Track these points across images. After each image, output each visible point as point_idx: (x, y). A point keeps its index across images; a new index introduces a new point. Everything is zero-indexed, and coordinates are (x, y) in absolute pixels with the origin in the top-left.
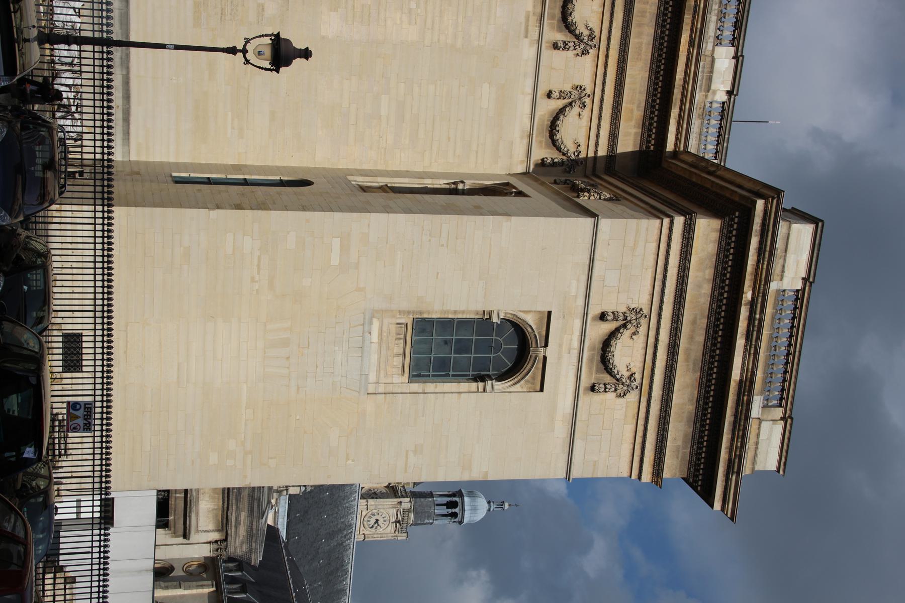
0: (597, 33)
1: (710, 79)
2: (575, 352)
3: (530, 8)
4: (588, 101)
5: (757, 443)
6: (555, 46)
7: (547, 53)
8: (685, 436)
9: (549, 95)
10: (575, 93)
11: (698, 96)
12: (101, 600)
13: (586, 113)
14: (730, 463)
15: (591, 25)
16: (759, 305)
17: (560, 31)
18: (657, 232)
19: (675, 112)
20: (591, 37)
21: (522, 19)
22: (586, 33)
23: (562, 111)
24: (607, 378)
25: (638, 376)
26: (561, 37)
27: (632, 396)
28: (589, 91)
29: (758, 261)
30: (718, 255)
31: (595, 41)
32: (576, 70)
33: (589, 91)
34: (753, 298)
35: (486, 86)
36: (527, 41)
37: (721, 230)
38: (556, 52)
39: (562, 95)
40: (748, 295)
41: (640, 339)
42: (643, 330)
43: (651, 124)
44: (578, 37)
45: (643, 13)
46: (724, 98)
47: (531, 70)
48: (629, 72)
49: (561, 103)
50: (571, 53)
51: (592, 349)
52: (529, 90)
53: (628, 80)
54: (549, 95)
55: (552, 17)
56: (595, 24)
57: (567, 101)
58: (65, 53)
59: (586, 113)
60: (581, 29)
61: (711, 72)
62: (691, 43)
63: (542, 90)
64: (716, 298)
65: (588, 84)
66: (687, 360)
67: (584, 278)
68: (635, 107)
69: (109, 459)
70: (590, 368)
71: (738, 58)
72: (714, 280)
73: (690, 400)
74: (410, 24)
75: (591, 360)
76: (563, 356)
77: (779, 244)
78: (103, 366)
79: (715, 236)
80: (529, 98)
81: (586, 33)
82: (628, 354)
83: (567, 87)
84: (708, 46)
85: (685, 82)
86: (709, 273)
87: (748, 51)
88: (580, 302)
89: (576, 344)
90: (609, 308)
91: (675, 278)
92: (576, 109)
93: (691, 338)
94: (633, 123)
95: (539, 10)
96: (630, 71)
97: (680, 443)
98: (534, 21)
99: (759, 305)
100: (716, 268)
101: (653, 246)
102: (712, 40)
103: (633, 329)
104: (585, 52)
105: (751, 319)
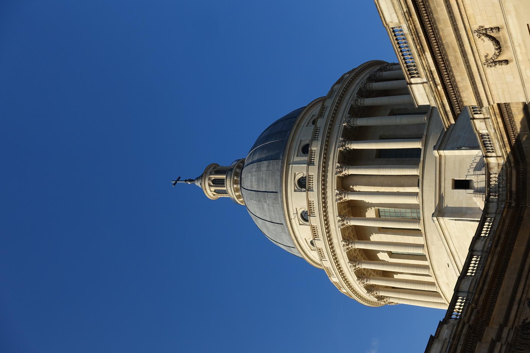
2: (516, 44)
5: (396, 13)
8: (437, 12)
14: (410, 15)
24: (492, 34)
25: (477, 37)
27: (475, 27)
41: (483, 54)
42: (483, 59)
51: (507, 47)
64: (451, 77)
66: (454, 49)
67: (525, 77)
70: (504, 38)
73: (442, 30)
75: (506, 42)
82: (487, 47)
88: (522, 67)
89: (517, 49)
90: (504, 66)
93: (456, 58)
97: (438, 9)
103: (489, 58)
105: (433, 79)
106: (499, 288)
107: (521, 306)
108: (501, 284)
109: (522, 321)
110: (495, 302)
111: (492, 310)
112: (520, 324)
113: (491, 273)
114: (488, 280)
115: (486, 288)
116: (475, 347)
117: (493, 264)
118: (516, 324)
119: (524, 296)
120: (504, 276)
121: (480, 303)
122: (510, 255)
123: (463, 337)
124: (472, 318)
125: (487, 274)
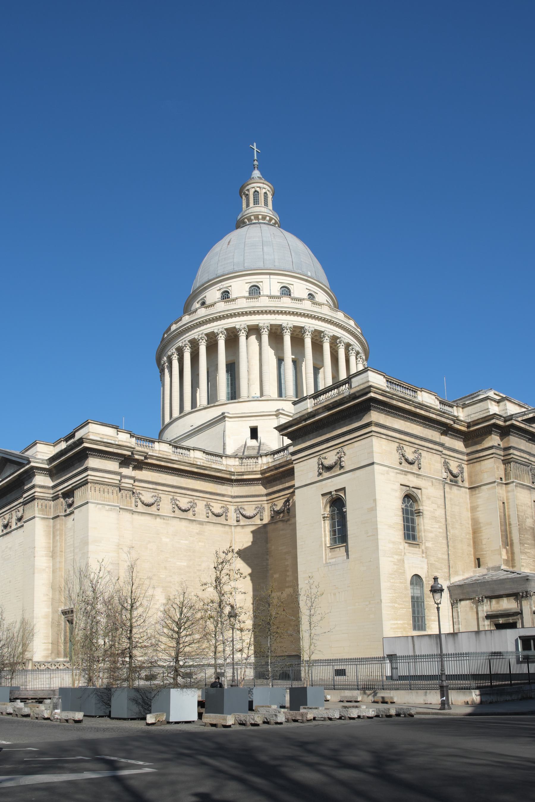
76: (332, 485)
107: (152, 490)
119: (160, 492)
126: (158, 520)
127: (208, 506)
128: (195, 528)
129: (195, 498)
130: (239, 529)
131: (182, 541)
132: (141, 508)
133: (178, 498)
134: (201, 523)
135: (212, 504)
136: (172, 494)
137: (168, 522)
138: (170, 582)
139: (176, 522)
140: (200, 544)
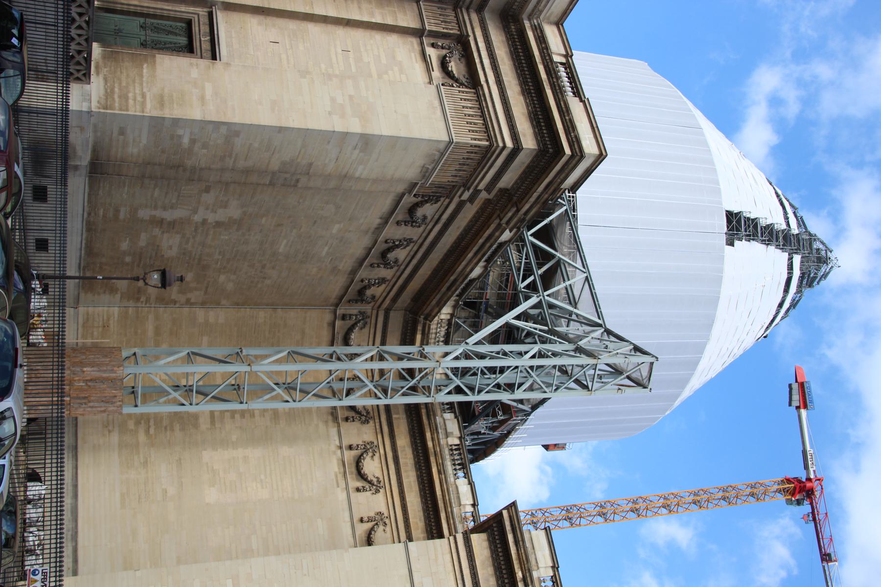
0: (381, 479)
1: (459, 498)
3: (336, 470)
4: (387, 521)
6: (358, 490)
7: (354, 495)
9: (362, 520)
10: (378, 518)
11: (455, 510)
12: (58, 583)
13: (388, 529)
15: (377, 475)
16: (529, 579)
17: (358, 481)
18: (447, 547)
19: (443, 515)
20: (379, 482)
21: (333, 477)
22: (375, 480)
23: (372, 529)
26: (360, 484)
28: (386, 515)
29: (518, 550)
30: (492, 556)
31: (382, 484)
32: (374, 503)
33: (386, 515)
34: (523, 576)
35: (319, 520)
36: (339, 490)
37: (488, 540)
38: (359, 494)
39: (370, 520)
40: (519, 575)
43: (431, 529)
44: (370, 482)
45: (406, 464)
46: (472, 509)
47: (346, 506)
48: (408, 499)
49: (370, 525)
50: (368, 493)
52: (348, 518)
53: (409, 504)
54: (362, 520)
55: (351, 473)
56: (378, 474)
57: (373, 523)
58: (34, 515)
59: (388, 529)
60: (370, 478)
61: (458, 493)
62: (439, 472)
63: (356, 518)
65: (384, 510)
68: (418, 520)
69: (63, 471)
71: (471, 484)
72: (496, 574)
74: (262, 488)
77: (528, 544)
78: (56, 538)
79: (486, 544)
80: (349, 524)
81: (375, 480)
83: (372, 514)
84: (451, 479)
85: (443, 496)
86: (490, 570)
87: (475, 478)
91: (469, 575)
92: (381, 527)
94: (420, 531)
95: (342, 470)
96: (408, 499)
98: (340, 477)
99: (529, 579)
100: (494, 565)
101: (449, 556)
102: (452, 476)
104: (377, 491)
106: (461, 234)
107: (436, 217)
108: (458, 238)
109: (439, 203)
110: (471, 221)
111: (477, 212)
112: (442, 199)
113: (470, 255)
114: (475, 249)
115: (481, 241)
116: (516, 182)
117: (464, 263)
118: (448, 200)
119: (429, 227)
120: (452, 247)
121: (493, 227)
122: (438, 266)
123: (532, 200)
124: (510, 214)
125: (476, 254)
126: (378, 221)
127: (383, 280)
128: (347, 264)
129: (403, 267)
130: (328, 317)
131: (326, 249)
132: (408, 200)
133: (408, 248)
134: (353, 272)
135: (384, 286)
136: (420, 241)
137: (370, 234)
138: (249, 230)
139: (366, 241)
140: (315, 270)
